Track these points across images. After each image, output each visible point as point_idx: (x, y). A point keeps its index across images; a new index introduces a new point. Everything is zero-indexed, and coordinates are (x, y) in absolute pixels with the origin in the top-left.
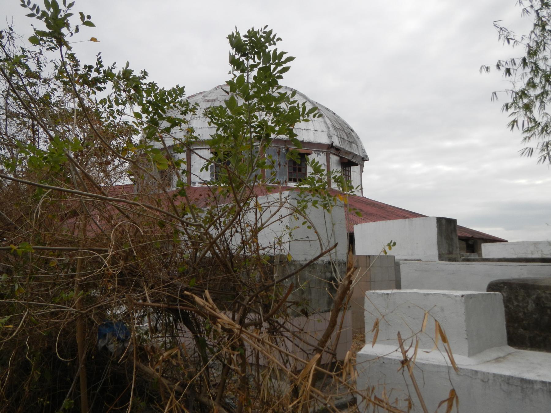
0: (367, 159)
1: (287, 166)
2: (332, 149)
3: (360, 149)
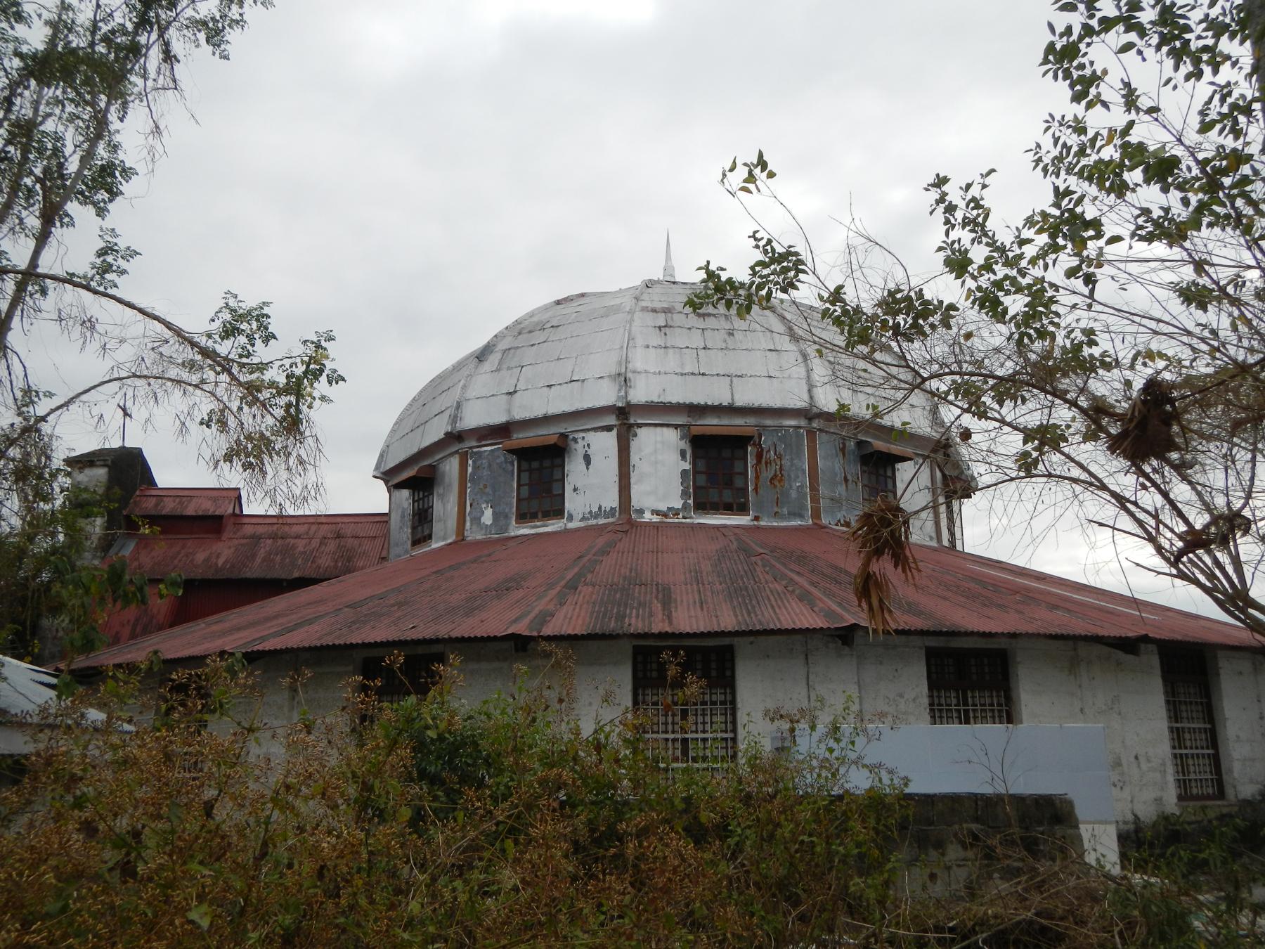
1: (860, 485)
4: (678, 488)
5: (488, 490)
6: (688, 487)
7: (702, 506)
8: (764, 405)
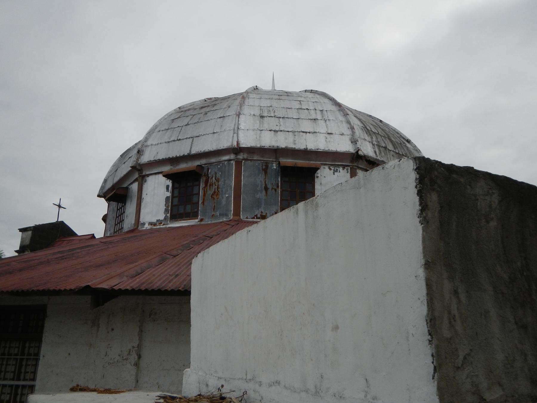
2: (360, 161)
6: (168, 207)
7: (174, 216)
8: (207, 150)
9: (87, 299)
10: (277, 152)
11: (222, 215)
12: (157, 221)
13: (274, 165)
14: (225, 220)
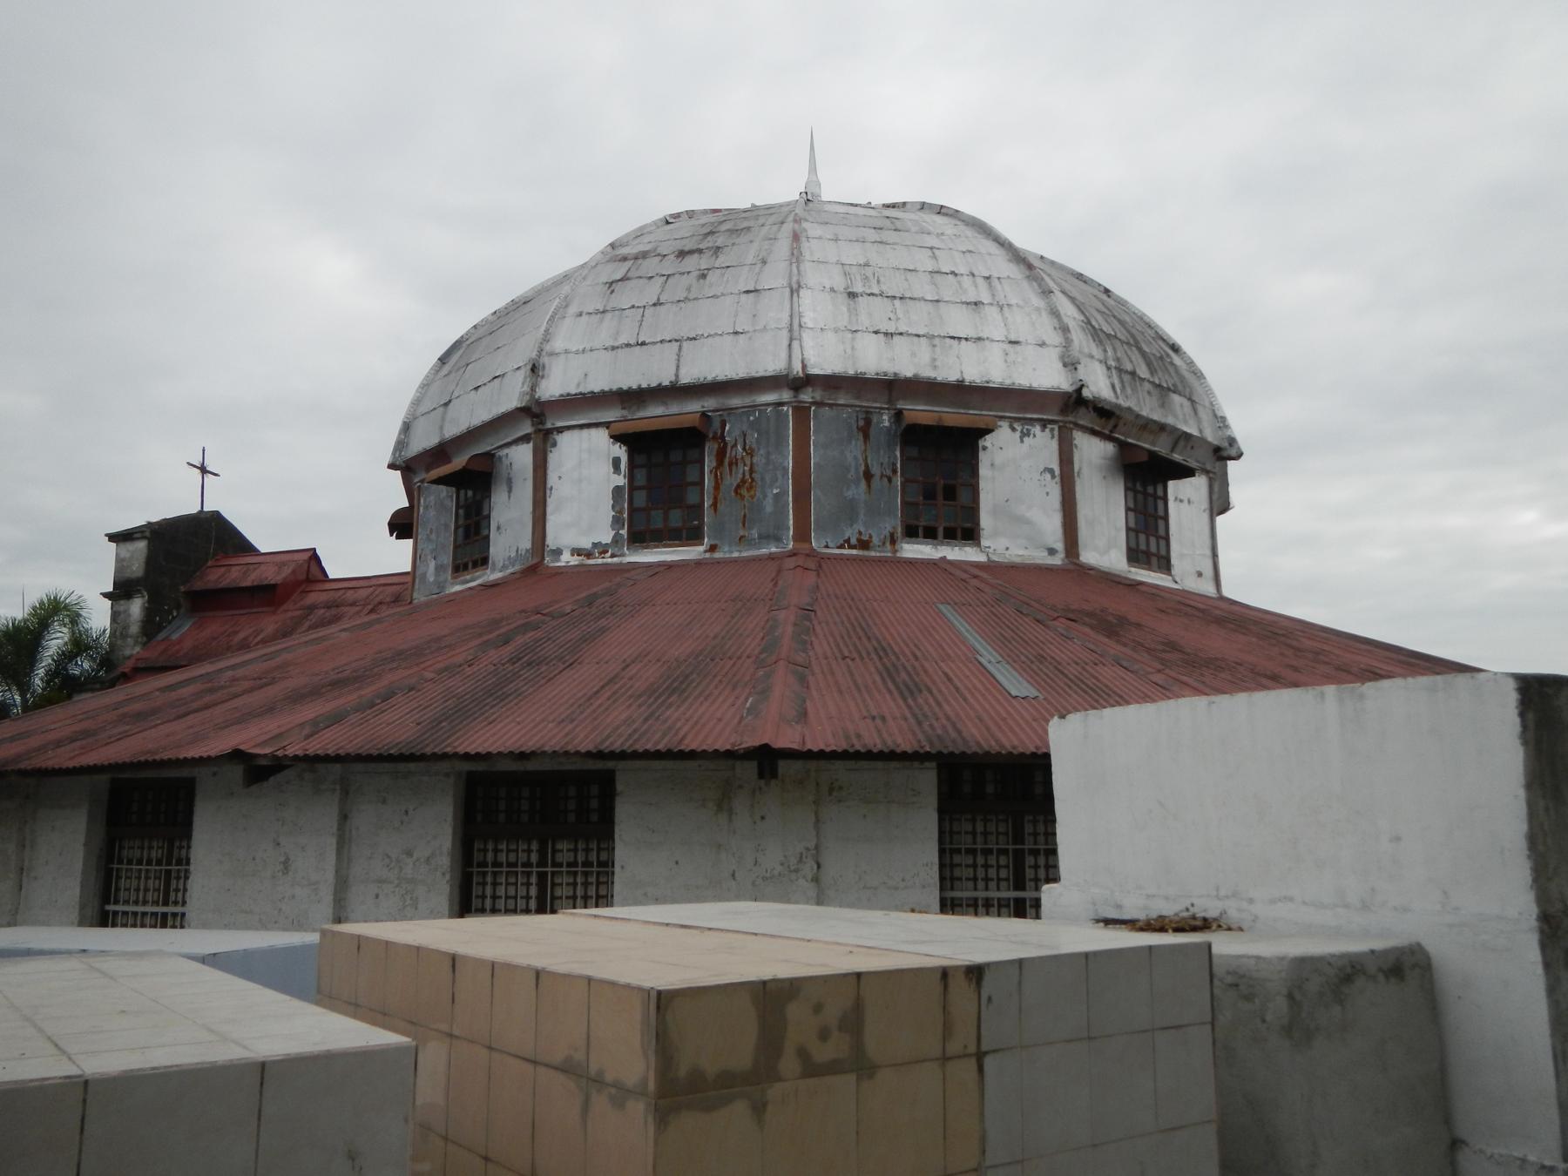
0: (1233, 452)
1: (898, 481)
2: (1082, 410)
3: (1204, 415)
4: (606, 513)
5: (433, 536)
6: (621, 512)
7: (640, 537)
8: (721, 377)
9: (751, 768)
10: (893, 387)
11: (766, 538)
12: (595, 545)
13: (885, 417)
14: (774, 550)
